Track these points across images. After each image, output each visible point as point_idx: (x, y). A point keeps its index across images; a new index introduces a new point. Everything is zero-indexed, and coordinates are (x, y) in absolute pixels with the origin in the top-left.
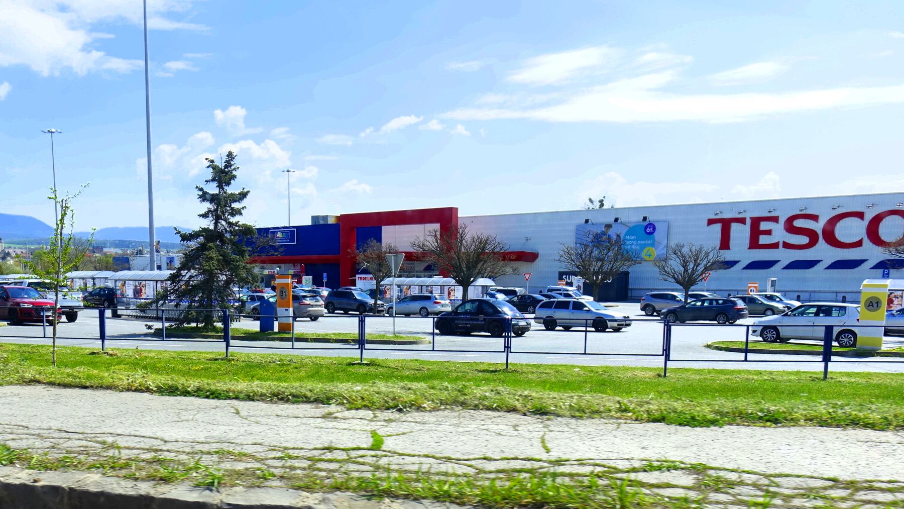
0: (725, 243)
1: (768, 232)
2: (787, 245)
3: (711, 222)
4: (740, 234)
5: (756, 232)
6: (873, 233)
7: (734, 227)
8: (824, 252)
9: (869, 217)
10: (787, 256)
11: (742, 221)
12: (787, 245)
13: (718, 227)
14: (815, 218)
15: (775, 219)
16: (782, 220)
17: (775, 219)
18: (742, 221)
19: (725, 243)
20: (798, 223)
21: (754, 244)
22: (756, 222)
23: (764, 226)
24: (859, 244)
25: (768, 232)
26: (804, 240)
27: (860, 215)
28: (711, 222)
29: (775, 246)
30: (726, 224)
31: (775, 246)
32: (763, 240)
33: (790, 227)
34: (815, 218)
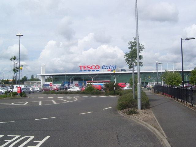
0: (81, 69)
3: (79, 66)
4: (82, 68)
8: (91, 70)
10: (87, 70)
15: (86, 66)
18: (82, 66)
19: (81, 69)
21: (84, 69)
22: (84, 66)
24: (94, 69)
27: (94, 66)
30: (81, 67)
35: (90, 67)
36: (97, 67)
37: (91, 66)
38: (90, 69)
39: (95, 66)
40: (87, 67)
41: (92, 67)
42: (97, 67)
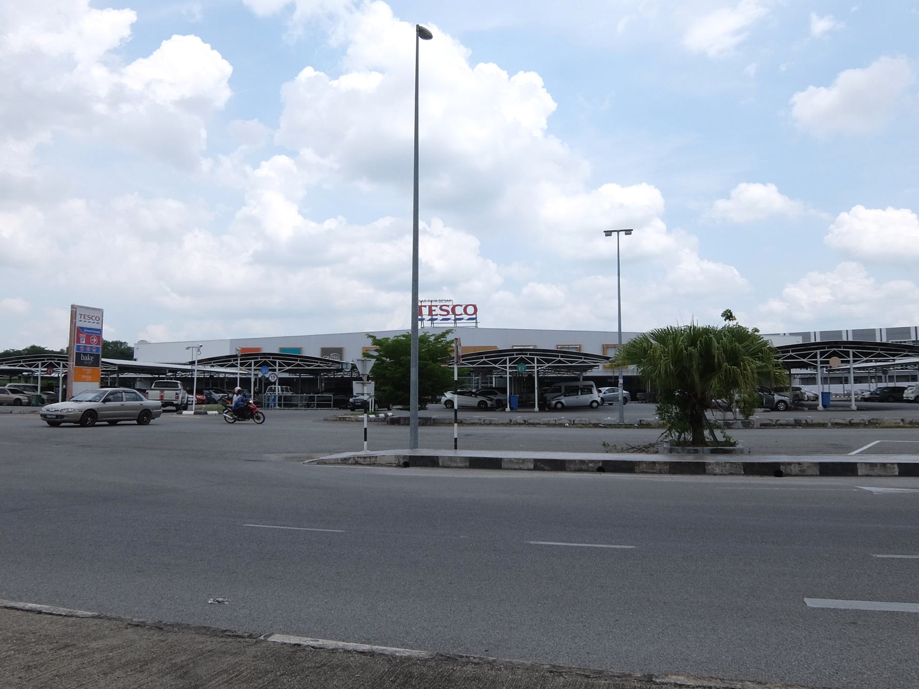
1: (435, 310)
2: (440, 315)
6: (465, 310)
7: (423, 308)
9: (463, 306)
11: (425, 306)
12: (440, 315)
14: (448, 306)
15: (436, 306)
16: (439, 307)
17: (436, 306)
18: (425, 306)
20: (443, 308)
23: (433, 308)
24: (461, 314)
25: (435, 310)
26: (446, 313)
27: (461, 306)
29: (437, 315)
31: (437, 315)
33: (441, 309)
34: (448, 306)
35: (449, 309)
36: (470, 310)
37: (451, 307)
38: (448, 314)
42: (470, 310)
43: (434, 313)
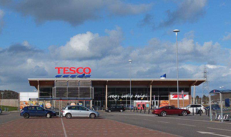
0: (59, 73)
1: (67, 70)
2: (70, 73)
3: (56, 68)
4: (62, 71)
5: (64, 70)
7: (60, 69)
10: (70, 75)
13: (57, 69)
14: (75, 68)
15: (68, 68)
17: (68, 68)
18: (62, 68)
19: (59, 73)
20: (72, 69)
21: (64, 73)
22: (64, 68)
23: (66, 69)
25: (67, 70)
26: (73, 72)
27: (82, 68)
28: (56, 68)
30: (59, 68)
31: (68, 73)
32: (66, 72)
33: (70, 70)
35: (75, 70)
37: (76, 69)
39: (84, 67)
40: (68, 70)
41: (78, 69)
43: (66, 72)
